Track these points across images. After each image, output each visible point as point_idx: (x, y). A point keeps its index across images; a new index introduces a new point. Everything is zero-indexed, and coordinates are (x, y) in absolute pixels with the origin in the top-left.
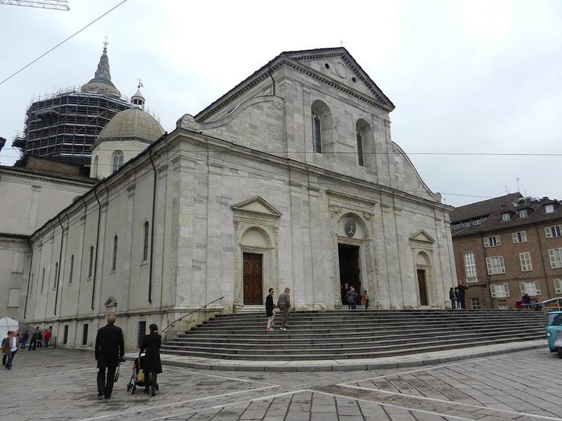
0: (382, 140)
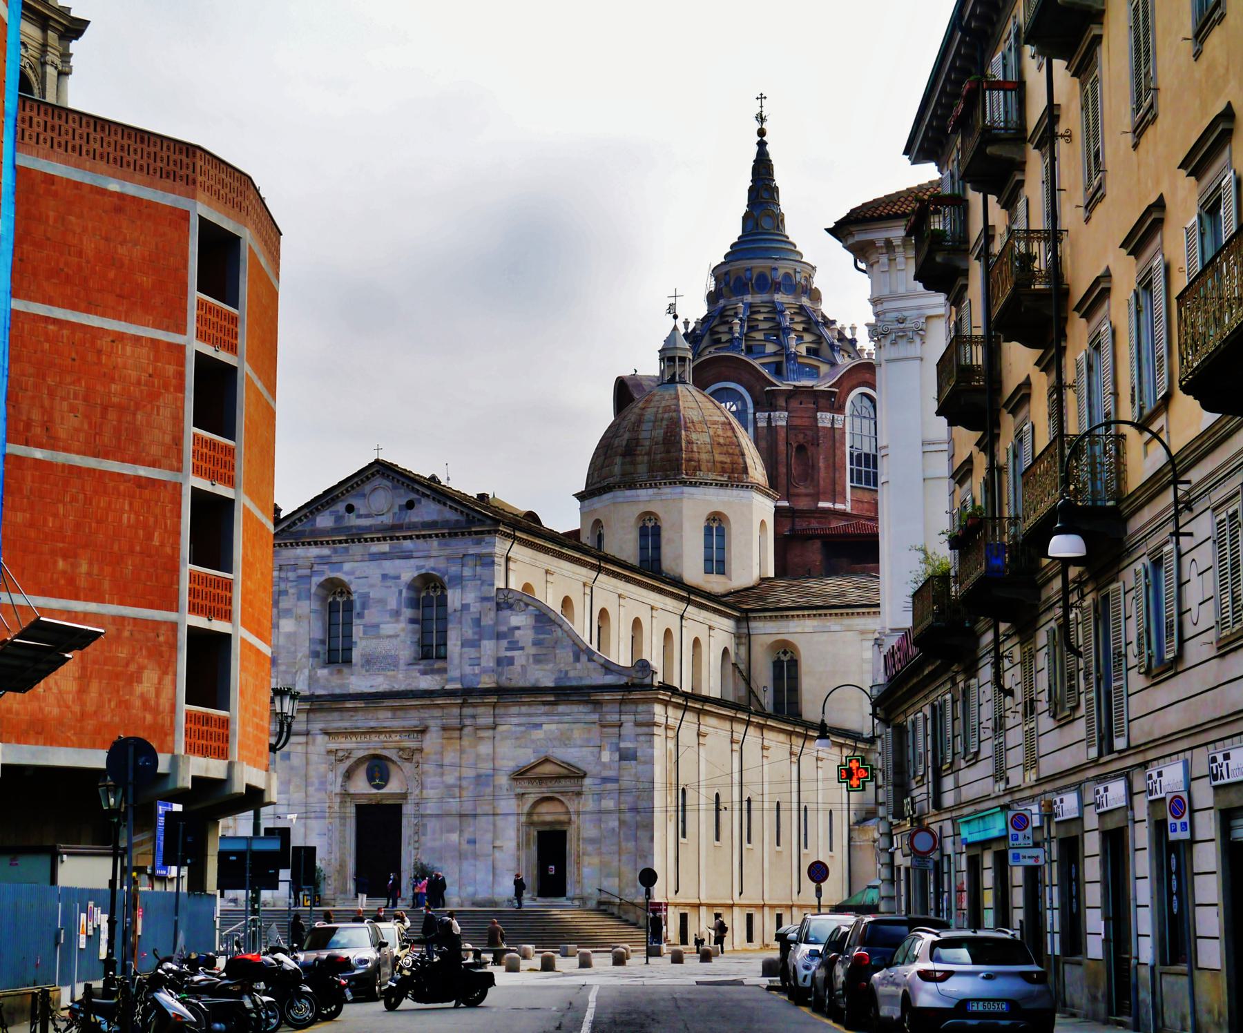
0: (470, 597)
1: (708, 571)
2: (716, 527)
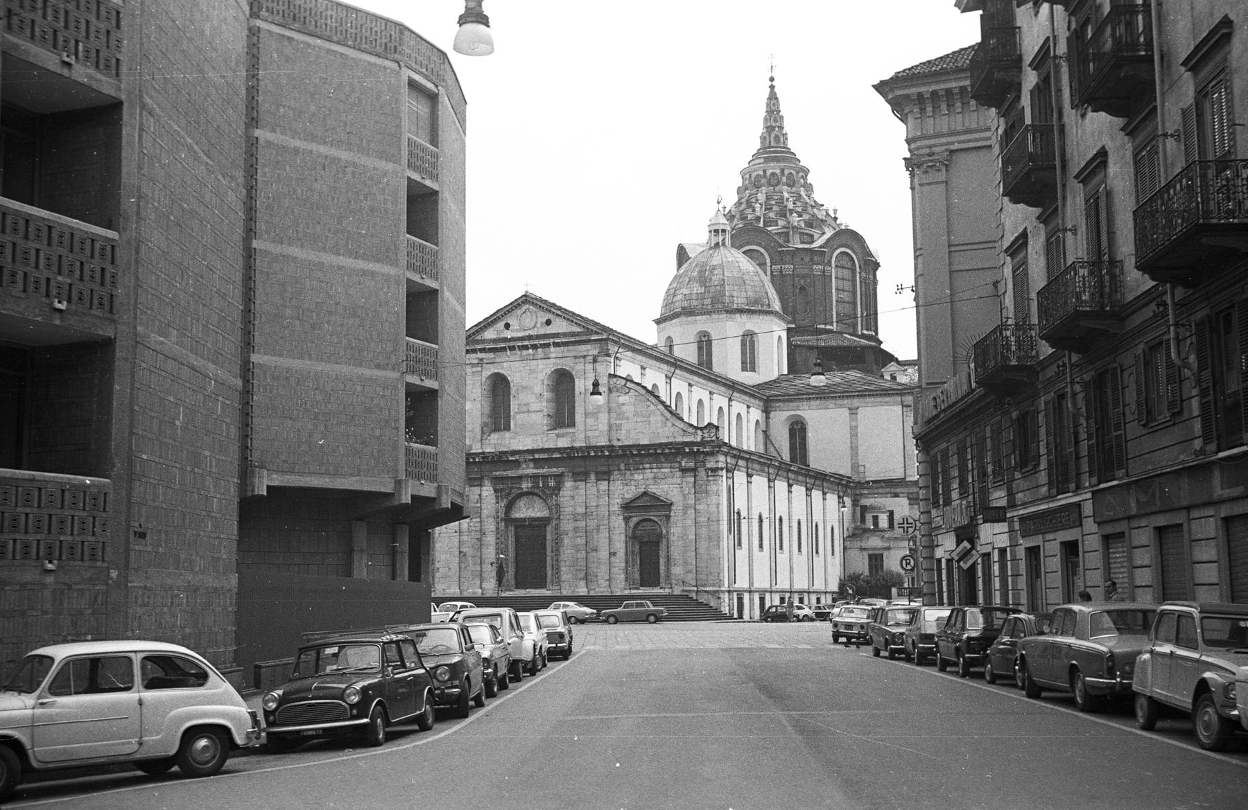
1: (744, 369)
2: (749, 342)
